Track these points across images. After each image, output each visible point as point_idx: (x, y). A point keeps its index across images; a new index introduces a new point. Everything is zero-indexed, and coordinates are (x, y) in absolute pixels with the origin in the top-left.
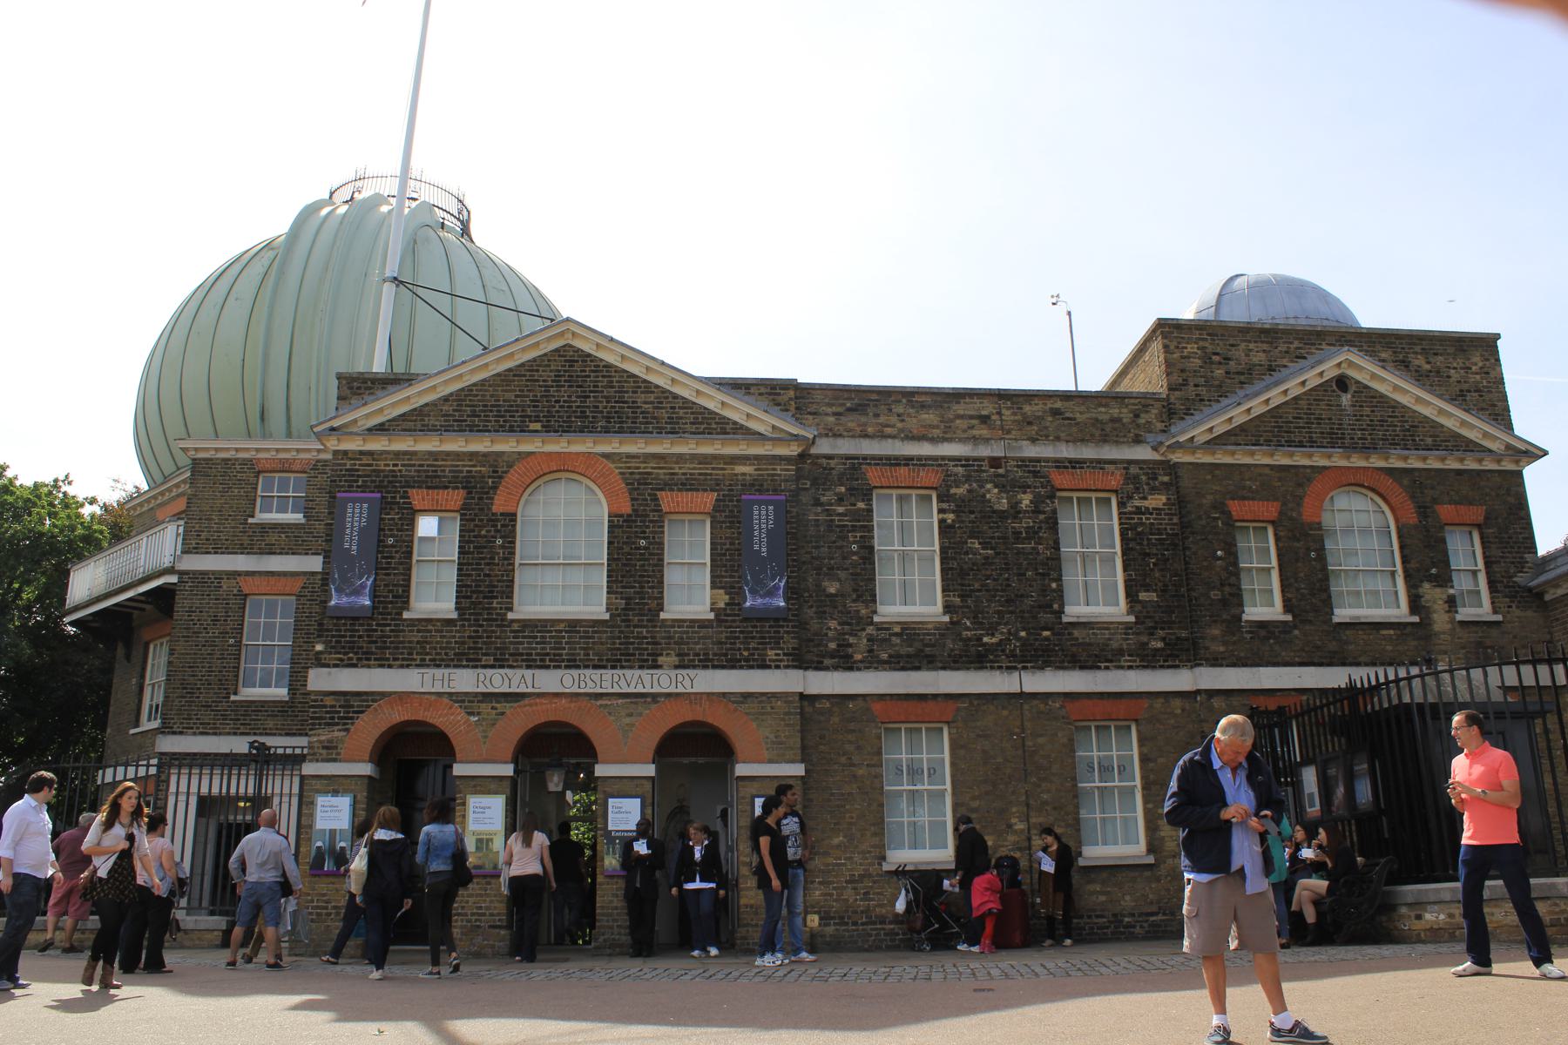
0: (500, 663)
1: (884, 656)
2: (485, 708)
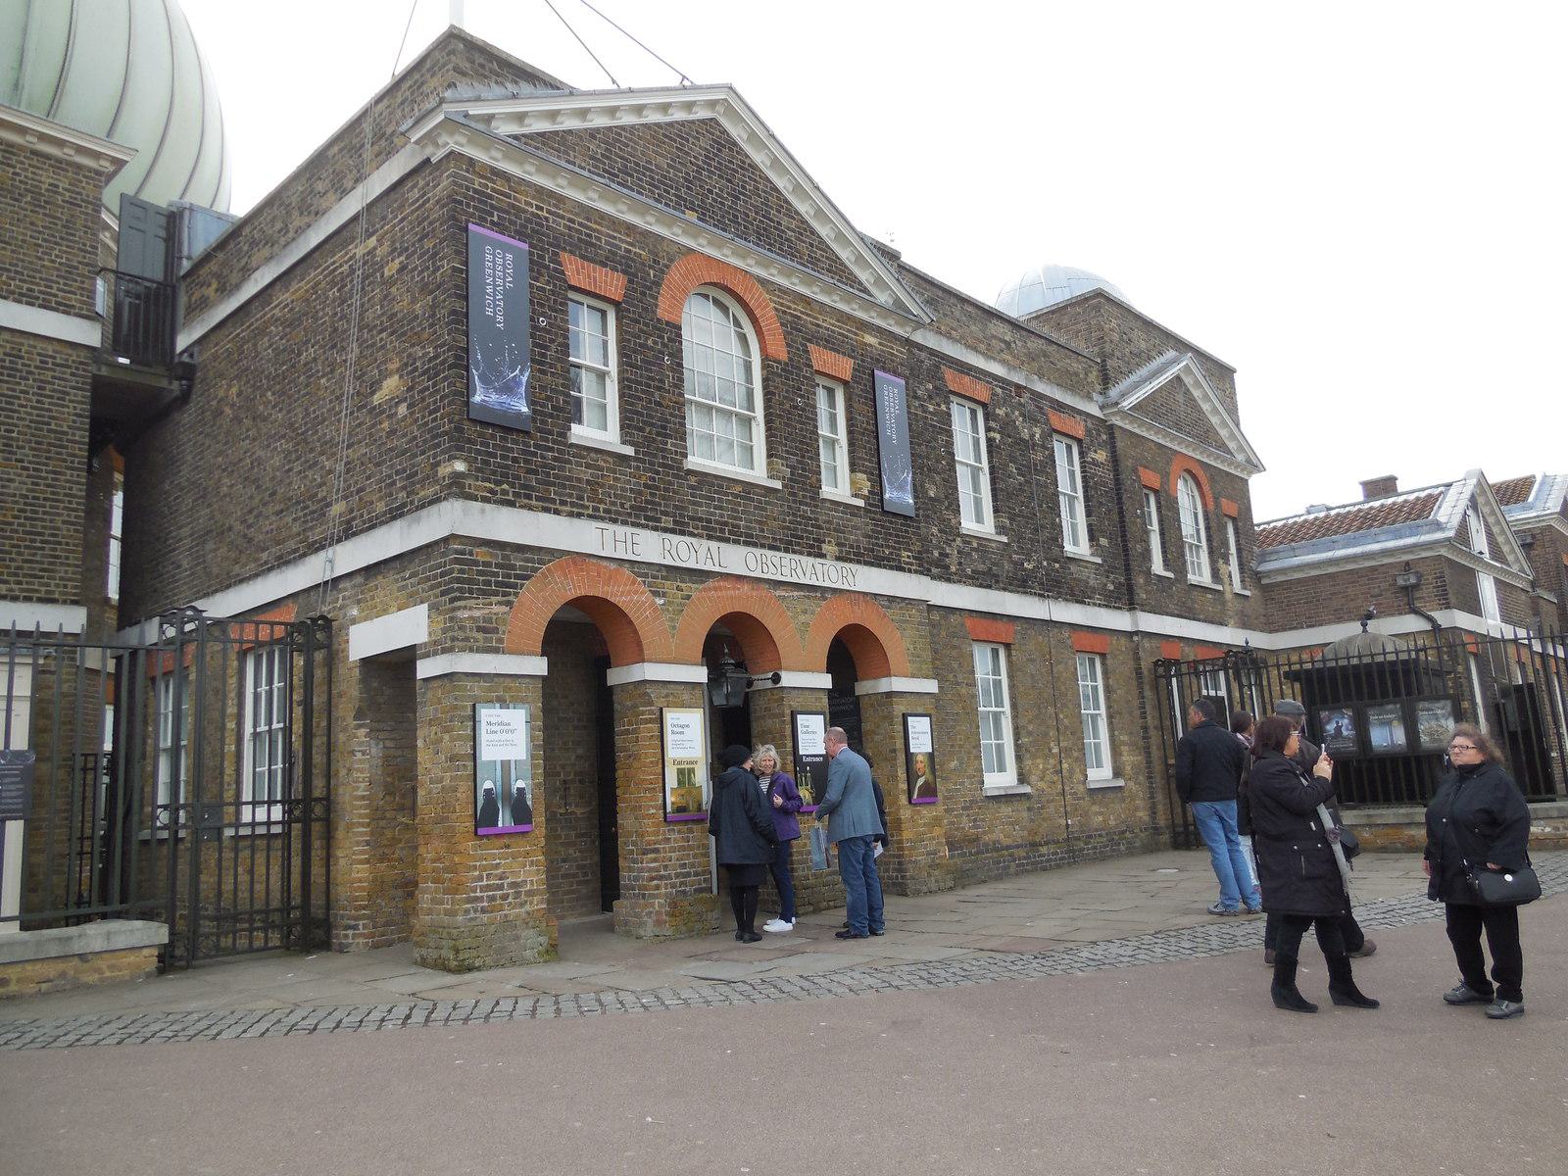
0: (679, 529)
1: (969, 571)
2: (669, 586)
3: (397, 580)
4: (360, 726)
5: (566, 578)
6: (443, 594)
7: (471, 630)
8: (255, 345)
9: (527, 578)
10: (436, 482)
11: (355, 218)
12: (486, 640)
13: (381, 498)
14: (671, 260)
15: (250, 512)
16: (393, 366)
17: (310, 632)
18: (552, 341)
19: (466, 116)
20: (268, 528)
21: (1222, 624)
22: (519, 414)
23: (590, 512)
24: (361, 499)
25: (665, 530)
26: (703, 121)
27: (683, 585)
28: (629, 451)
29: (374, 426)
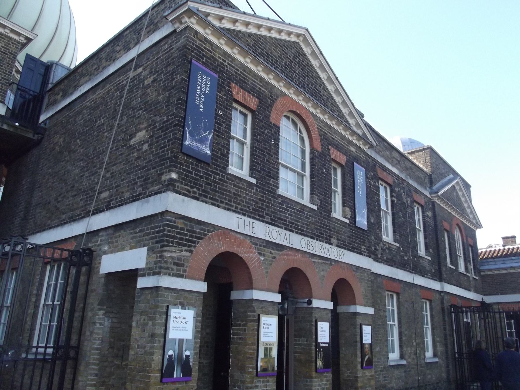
0: (272, 223)
2: (267, 251)
3: (131, 233)
4: (100, 309)
5: (220, 240)
6: (157, 242)
7: (171, 263)
8: (75, 119)
9: (201, 239)
10: (160, 183)
11: (132, 60)
12: (177, 270)
13: (128, 191)
14: (278, 97)
15: (60, 195)
16: (145, 125)
17: (81, 257)
18: (224, 122)
19: (198, 10)
20: (68, 203)
21: (469, 290)
22: (206, 154)
23: (234, 209)
24: (117, 191)
25: (267, 223)
26: (293, 42)
27: (273, 251)
28: (254, 181)
29: (129, 155)
